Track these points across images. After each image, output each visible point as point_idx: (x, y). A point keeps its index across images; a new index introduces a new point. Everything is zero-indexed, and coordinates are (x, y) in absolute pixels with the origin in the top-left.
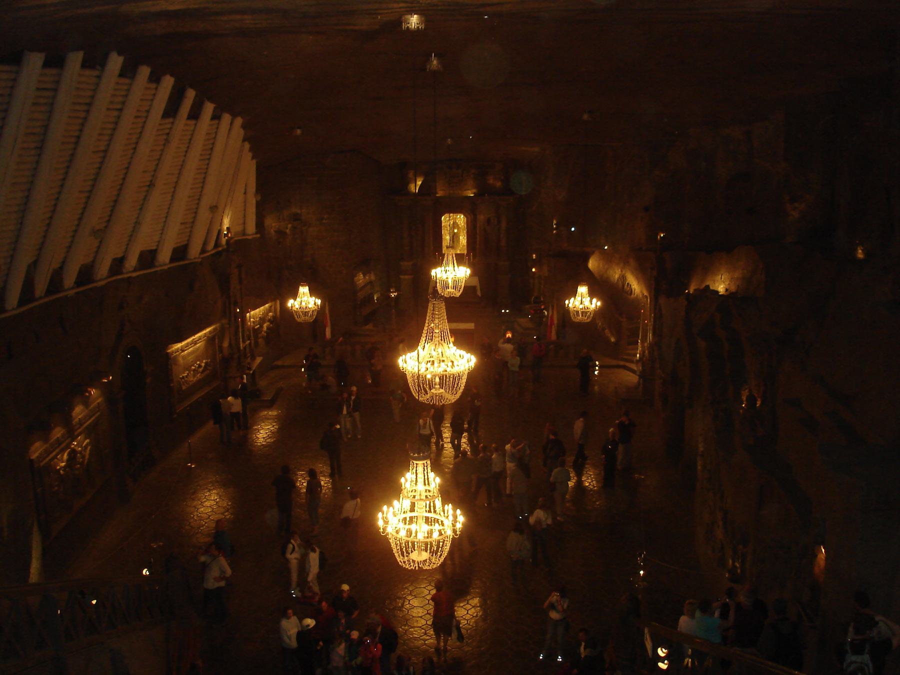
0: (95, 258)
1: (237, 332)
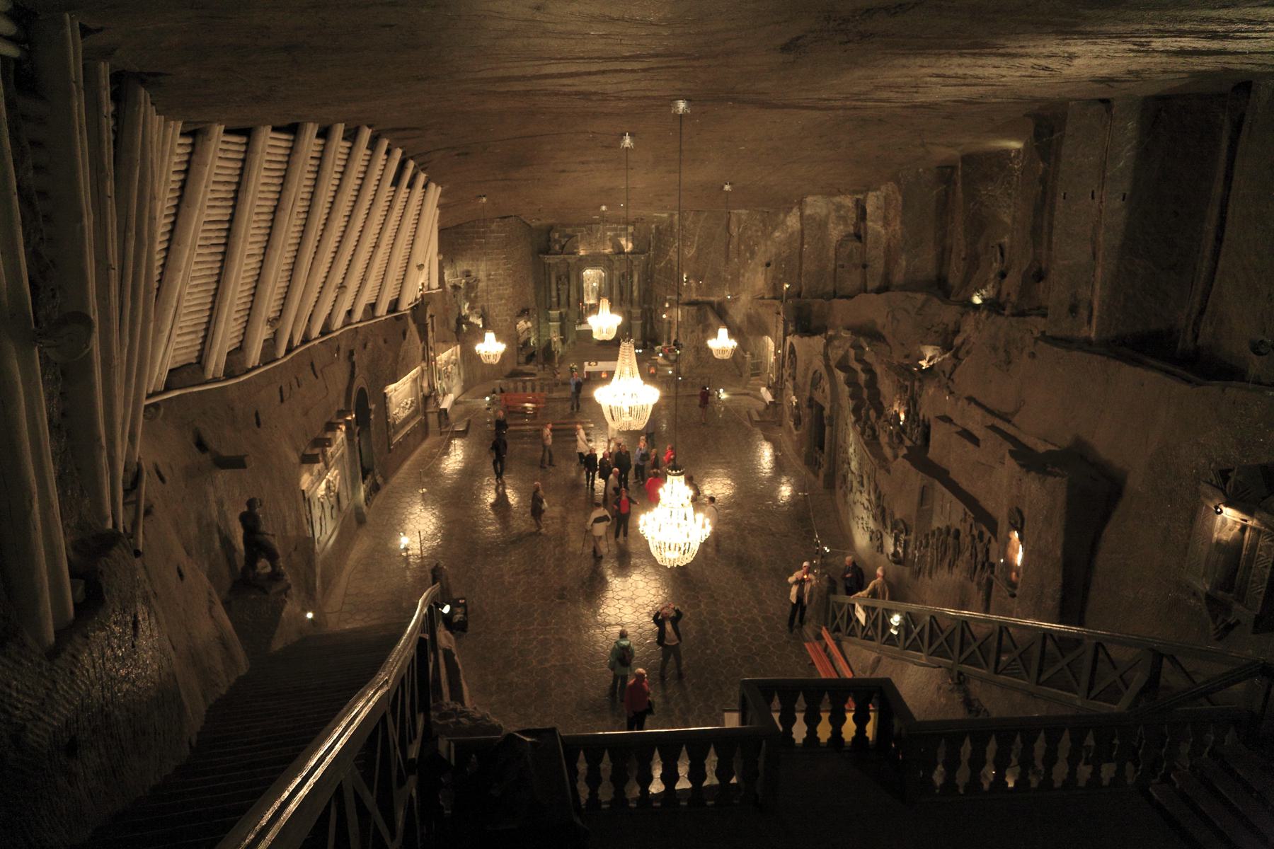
0: (332, 310)
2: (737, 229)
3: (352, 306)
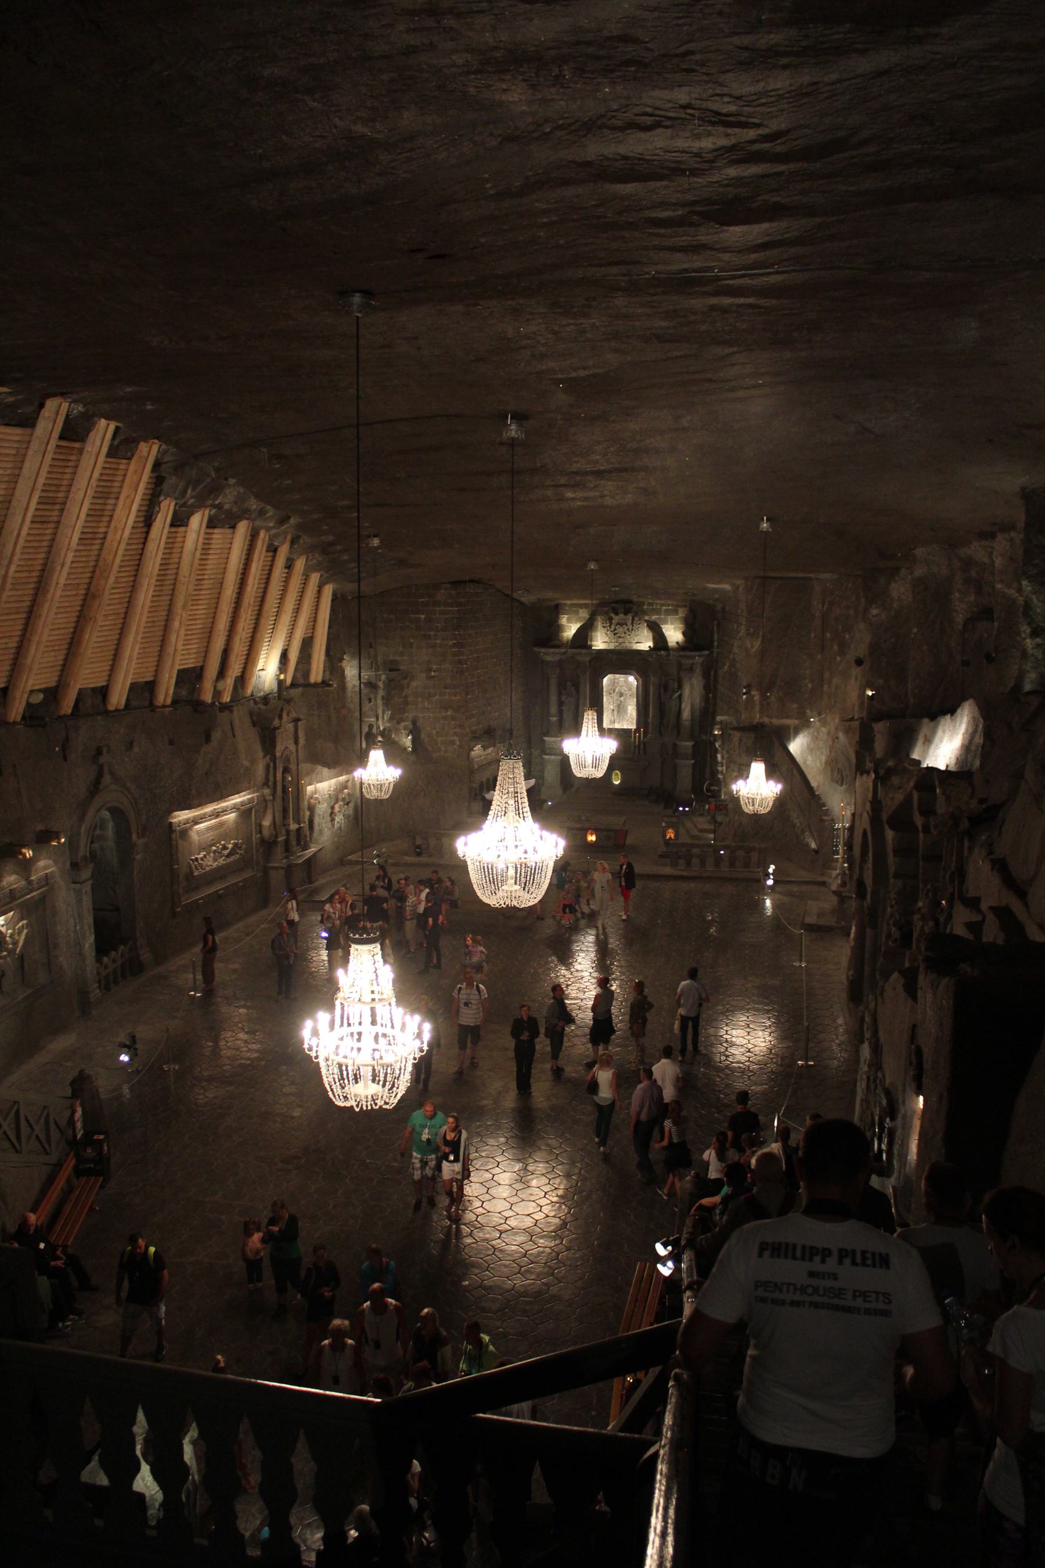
1: (285, 810)
2: (820, 606)
3: (109, 681)
